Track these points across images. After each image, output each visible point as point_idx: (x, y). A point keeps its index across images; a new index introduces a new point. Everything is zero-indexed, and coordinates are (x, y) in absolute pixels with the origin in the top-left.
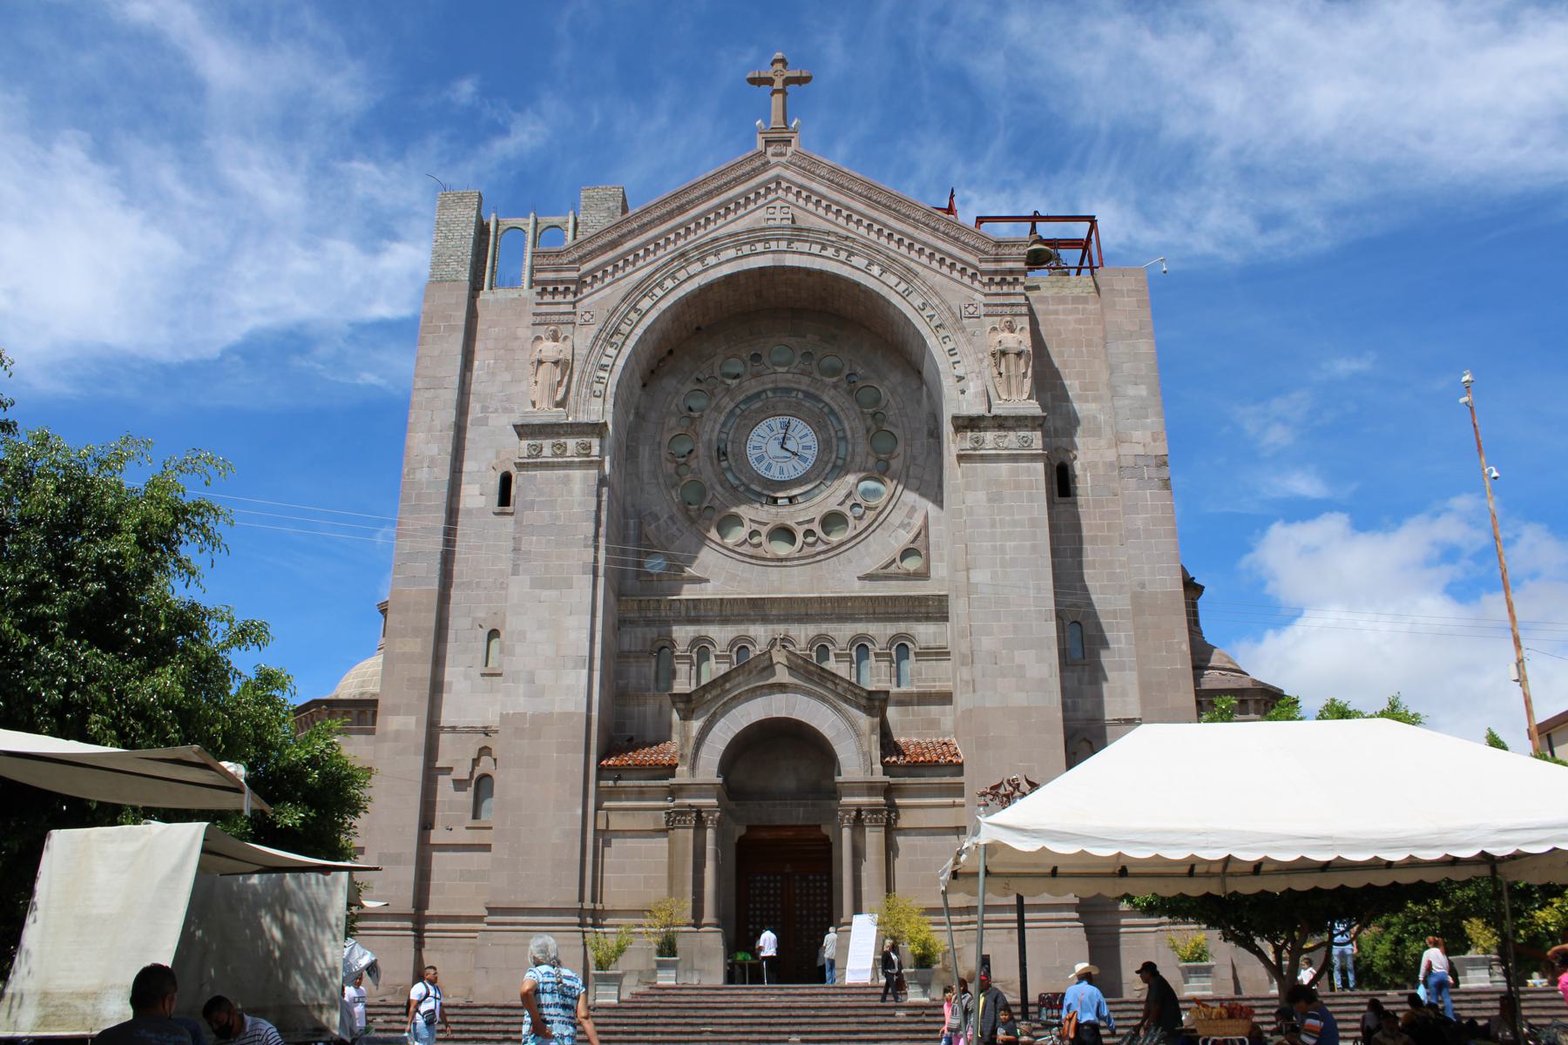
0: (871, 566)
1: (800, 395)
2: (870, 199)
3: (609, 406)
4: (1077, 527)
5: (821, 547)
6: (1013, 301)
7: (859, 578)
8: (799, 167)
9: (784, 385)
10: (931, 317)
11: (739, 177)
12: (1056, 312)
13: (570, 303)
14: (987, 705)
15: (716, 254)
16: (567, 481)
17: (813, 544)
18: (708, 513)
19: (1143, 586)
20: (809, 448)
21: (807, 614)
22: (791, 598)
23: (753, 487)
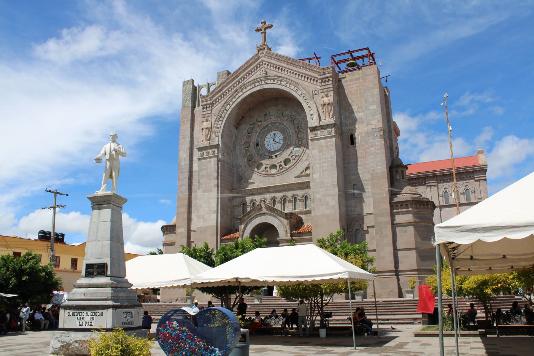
0: (297, 173)
1: (278, 124)
2: (287, 62)
3: (220, 139)
4: (356, 154)
5: (284, 169)
6: (328, 87)
7: (294, 177)
8: (268, 56)
9: (273, 122)
10: (304, 97)
11: (252, 63)
12: (350, 85)
13: (210, 110)
14: (318, 214)
15: (246, 89)
16: (210, 161)
17: (282, 169)
18: (254, 163)
19: (374, 171)
21: (280, 190)
22: (275, 186)
23: (266, 154)
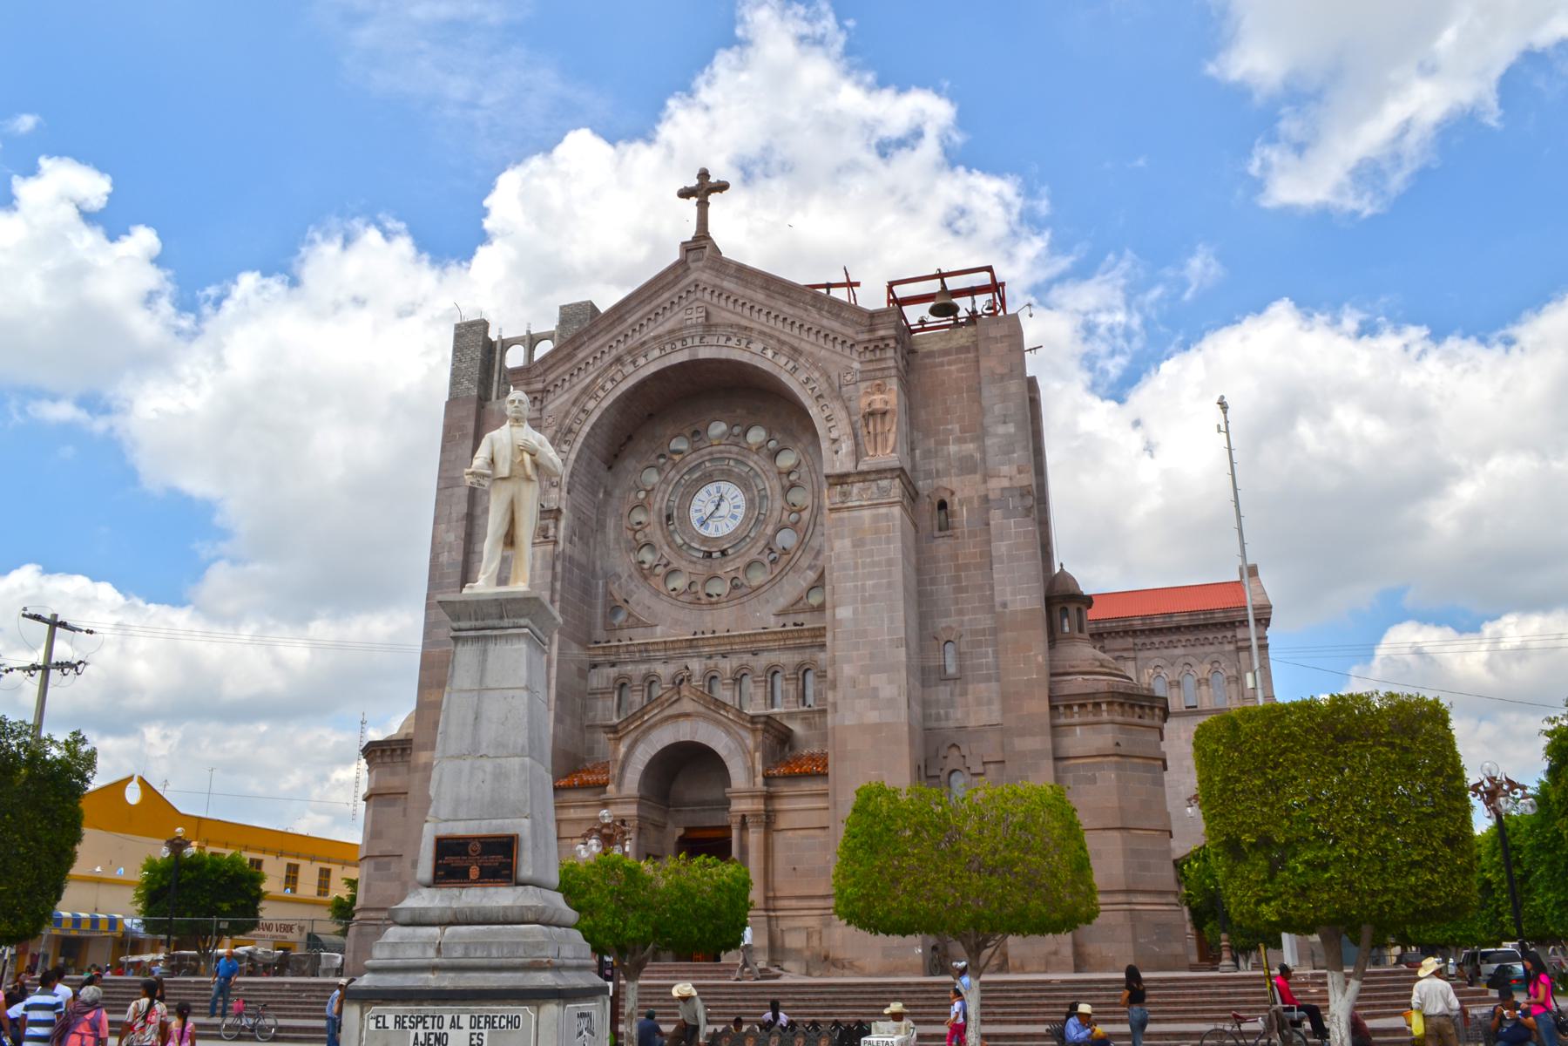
0: (783, 602)
3: (564, 494)
10: (813, 389)
12: (942, 364)
14: (847, 723)
20: (738, 507)
23: (693, 544)
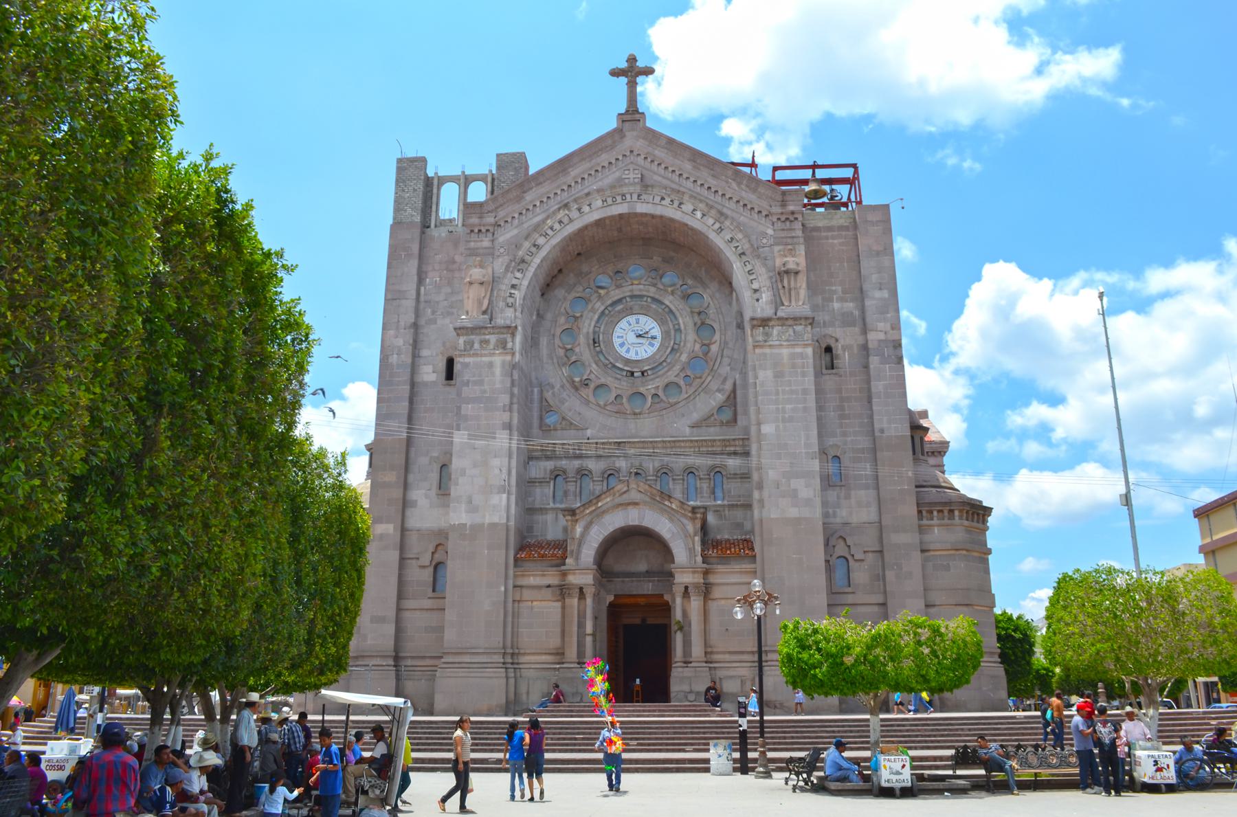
0: (696, 416)
3: (518, 314)
10: (736, 247)
12: (827, 238)
14: (772, 516)
23: (618, 365)
